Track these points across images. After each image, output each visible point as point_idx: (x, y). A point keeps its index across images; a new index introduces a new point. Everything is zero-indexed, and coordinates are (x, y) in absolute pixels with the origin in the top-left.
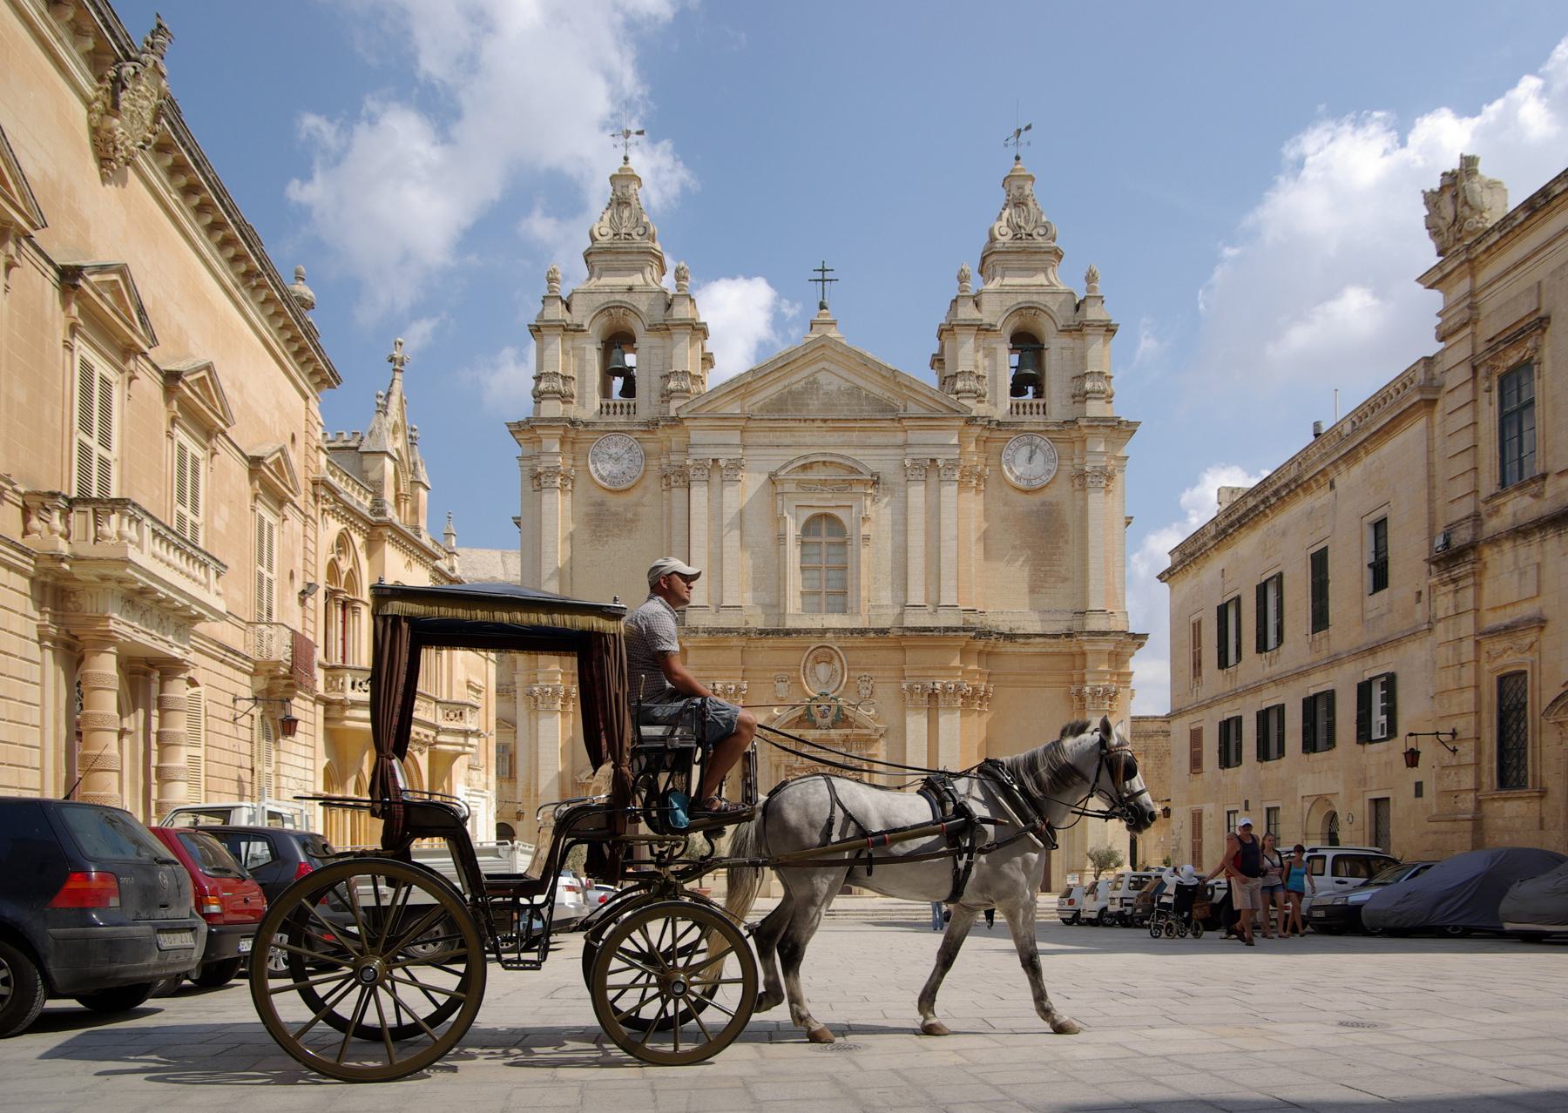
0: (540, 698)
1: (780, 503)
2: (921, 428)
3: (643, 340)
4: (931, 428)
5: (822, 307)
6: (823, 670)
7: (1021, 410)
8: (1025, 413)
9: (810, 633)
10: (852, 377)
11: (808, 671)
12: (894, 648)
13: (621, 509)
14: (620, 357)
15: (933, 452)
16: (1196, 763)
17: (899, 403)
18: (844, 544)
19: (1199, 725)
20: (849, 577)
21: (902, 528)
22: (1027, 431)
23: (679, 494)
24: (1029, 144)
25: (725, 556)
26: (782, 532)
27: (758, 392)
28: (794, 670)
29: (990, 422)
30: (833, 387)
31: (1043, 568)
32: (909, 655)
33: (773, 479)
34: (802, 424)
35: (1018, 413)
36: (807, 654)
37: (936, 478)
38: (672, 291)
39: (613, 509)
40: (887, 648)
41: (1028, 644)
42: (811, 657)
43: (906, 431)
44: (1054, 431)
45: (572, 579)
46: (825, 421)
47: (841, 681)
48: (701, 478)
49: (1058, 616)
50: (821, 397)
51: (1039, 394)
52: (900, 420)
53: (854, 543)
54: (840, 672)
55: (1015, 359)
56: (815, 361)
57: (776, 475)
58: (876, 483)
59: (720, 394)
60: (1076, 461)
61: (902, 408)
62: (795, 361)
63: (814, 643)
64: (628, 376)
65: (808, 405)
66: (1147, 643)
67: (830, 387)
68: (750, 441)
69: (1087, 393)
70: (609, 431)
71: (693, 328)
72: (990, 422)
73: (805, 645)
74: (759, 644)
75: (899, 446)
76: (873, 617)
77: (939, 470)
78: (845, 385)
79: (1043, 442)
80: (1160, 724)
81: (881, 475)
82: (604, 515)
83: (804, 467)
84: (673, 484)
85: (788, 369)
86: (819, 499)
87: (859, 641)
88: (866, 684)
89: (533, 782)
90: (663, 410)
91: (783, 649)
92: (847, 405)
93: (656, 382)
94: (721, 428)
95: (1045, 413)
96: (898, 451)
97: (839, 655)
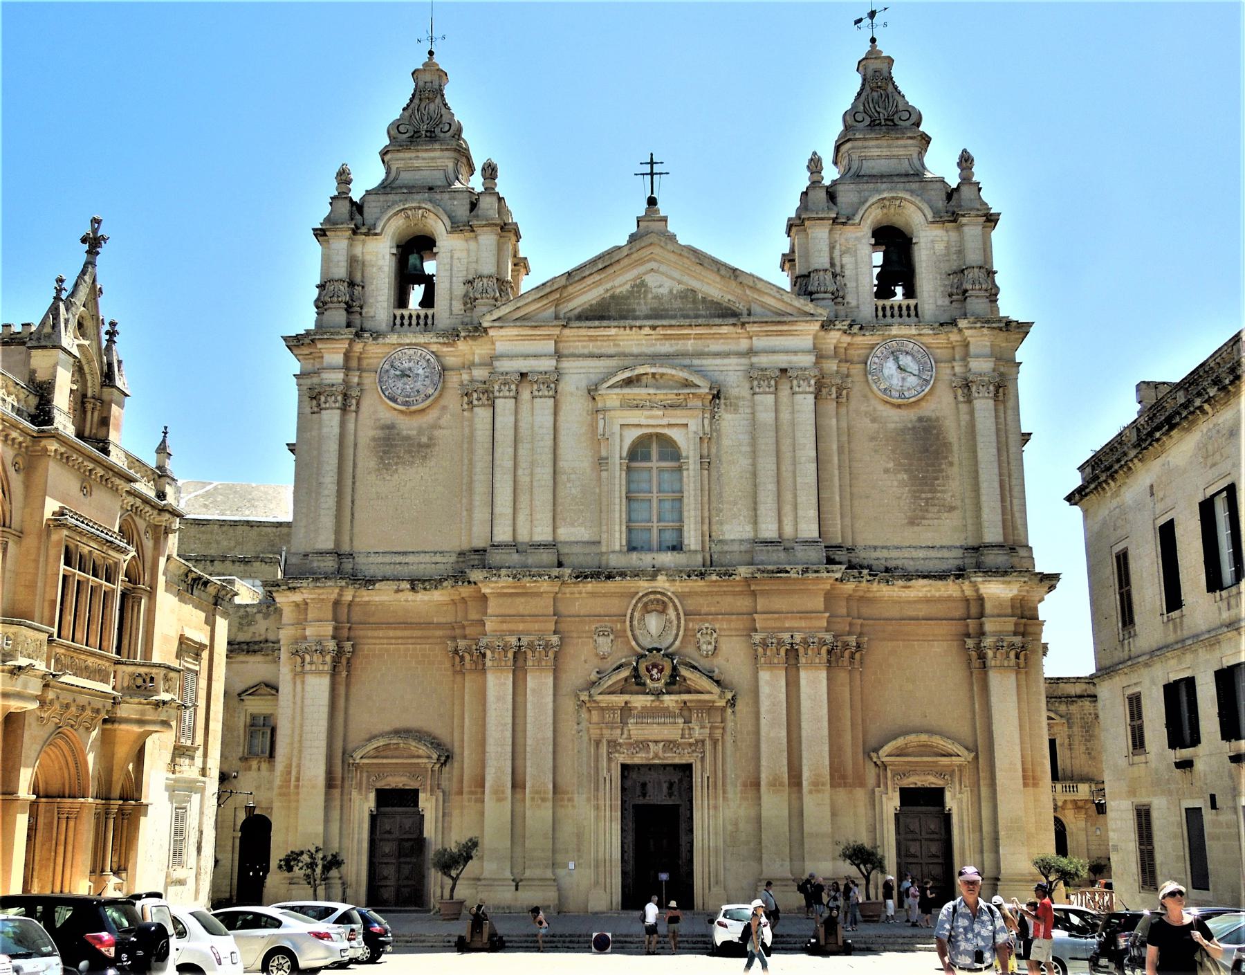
0: (307, 658)
1: (601, 423)
2: (768, 334)
3: (447, 242)
4: (781, 333)
5: (652, 202)
6: (653, 623)
7: (888, 313)
8: (892, 316)
9: (637, 575)
10: (686, 279)
11: (635, 623)
12: (741, 593)
13: (415, 433)
14: (418, 262)
15: (782, 360)
16: (1138, 741)
17: (741, 307)
18: (680, 469)
19: (1137, 689)
20: (685, 508)
21: (747, 449)
22: (895, 336)
23: (482, 414)
24: (885, 25)
25: (535, 484)
26: (604, 454)
27: (577, 296)
28: (617, 621)
29: (851, 326)
30: (664, 291)
31: (923, 496)
32: (761, 603)
33: (592, 392)
34: (628, 331)
35: (884, 316)
36: (634, 601)
37: (789, 391)
38: (479, 188)
39: (405, 433)
40: (734, 594)
41: (909, 587)
42: (640, 605)
43: (751, 338)
44: (929, 335)
45: (353, 514)
46: (654, 328)
47: (677, 635)
48: (507, 394)
49: (946, 554)
50: (649, 301)
51: (910, 293)
52: (743, 324)
53: (691, 467)
54: (675, 622)
55: (878, 258)
56: (641, 262)
57: (596, 390)
58: (717, 396)
59: (530, 299)
60: (958, 369)
61: (745, 312)
62: (618, 261)
63: (643, 585)
64: (429, 282)
65: (634, 310)
66: (1059, 585)
67: (661, 290)
68: (566, 352)
69: (966, 291)
70: (401, 345)
71: (502, 228)
72: (851, 326)
73: (633, 590)
74: (576, 590)
75: (740, 354)
76: (715, 557)
77: (791, 381)
78: (677, 288)
79: (916, 347)
80: (1084, 686)
81: (723, 389)
82: (394, 440)
83: (629, 382)
84: (475, 402)
85: (610, 270)
86: (647, 417)
87: (697, 584)
88: (708, 638)
89: (294, 764)
90: (466, 320)
91: (604, 595)
92: (680, 309)
93: (460, 290)
94: (531, 338)
95: (917, 315)
96: (744, 361)
97: (673, 602)
